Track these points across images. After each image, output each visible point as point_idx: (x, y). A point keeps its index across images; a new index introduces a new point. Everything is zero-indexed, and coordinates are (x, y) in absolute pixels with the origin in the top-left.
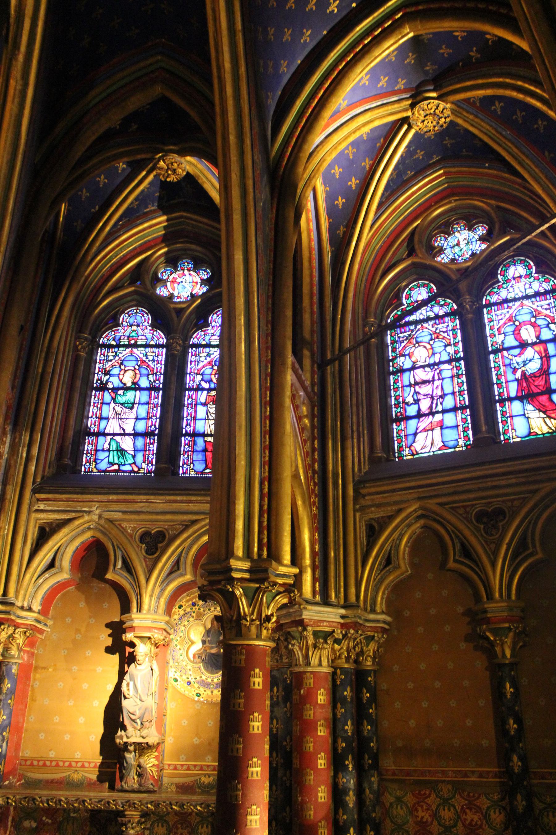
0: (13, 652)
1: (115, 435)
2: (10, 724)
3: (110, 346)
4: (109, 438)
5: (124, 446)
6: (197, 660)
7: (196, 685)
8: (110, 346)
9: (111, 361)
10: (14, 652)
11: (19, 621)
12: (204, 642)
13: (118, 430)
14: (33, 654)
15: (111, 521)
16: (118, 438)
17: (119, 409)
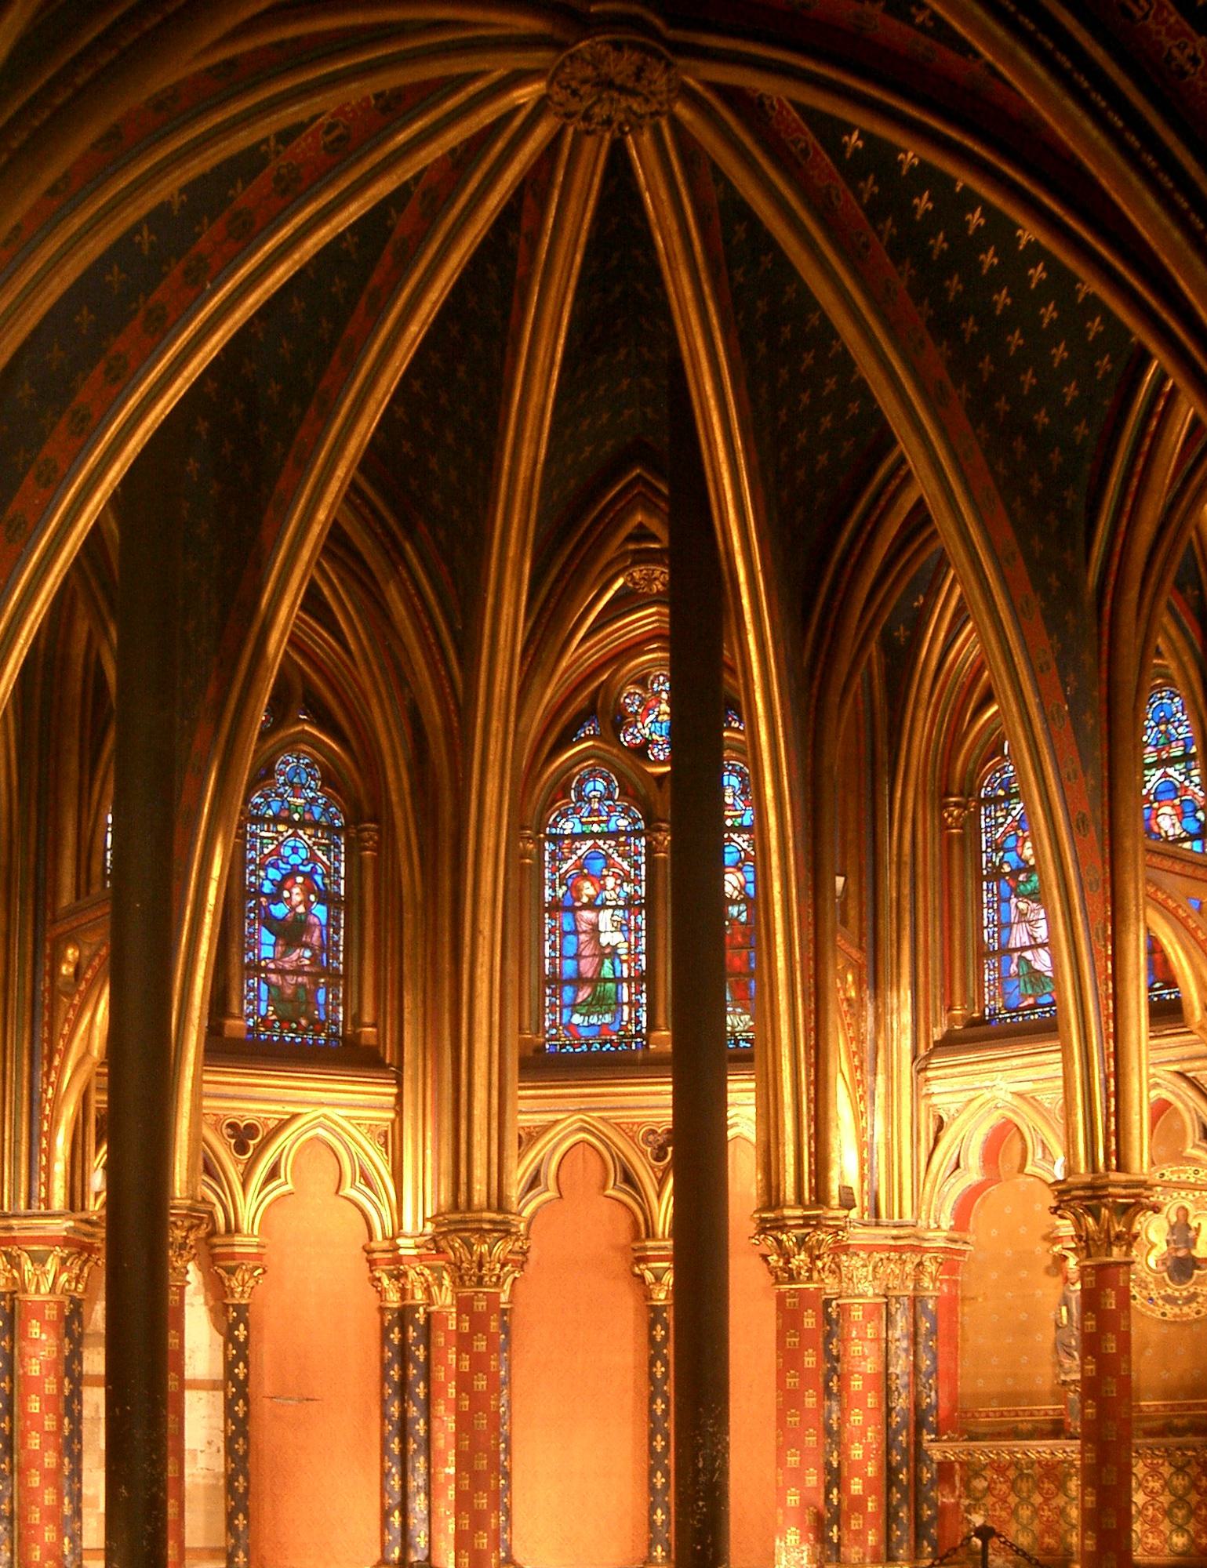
0: (926, 1285)
1: (1023, 949)
2: (936, 1370)
3: (997, 800)
4: (1016, 955)
5: (1037, 966)
6: (1161, 1268)
7: (1160, 1302)
8: (997, 800)
9: (1002, 824)
10: (926, 1282)
11: (926, 1245)
12: (1168, 1242)
13: (1026, 941)
14: (956, 1282)
15: (1019, 1095)
16: (1028, 955)
17: (1022, 906)
